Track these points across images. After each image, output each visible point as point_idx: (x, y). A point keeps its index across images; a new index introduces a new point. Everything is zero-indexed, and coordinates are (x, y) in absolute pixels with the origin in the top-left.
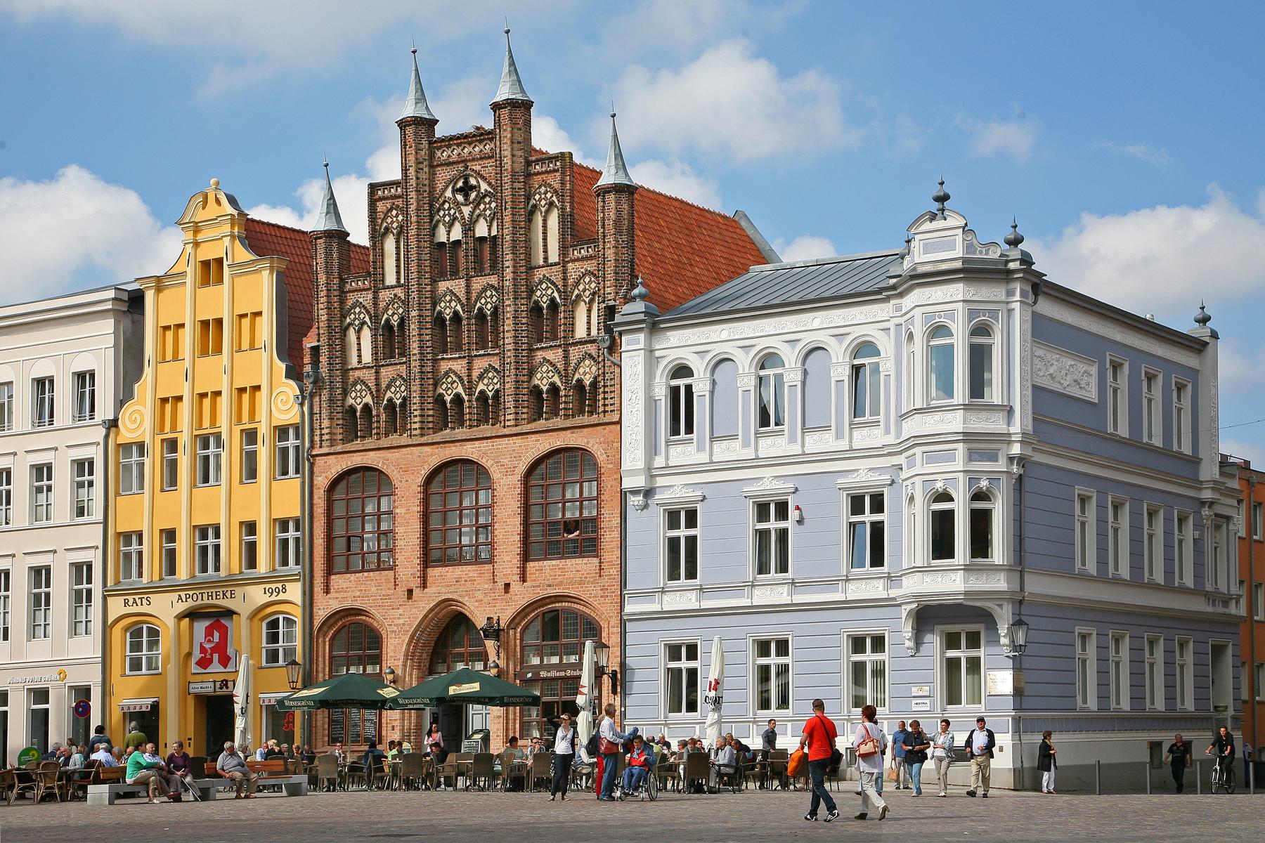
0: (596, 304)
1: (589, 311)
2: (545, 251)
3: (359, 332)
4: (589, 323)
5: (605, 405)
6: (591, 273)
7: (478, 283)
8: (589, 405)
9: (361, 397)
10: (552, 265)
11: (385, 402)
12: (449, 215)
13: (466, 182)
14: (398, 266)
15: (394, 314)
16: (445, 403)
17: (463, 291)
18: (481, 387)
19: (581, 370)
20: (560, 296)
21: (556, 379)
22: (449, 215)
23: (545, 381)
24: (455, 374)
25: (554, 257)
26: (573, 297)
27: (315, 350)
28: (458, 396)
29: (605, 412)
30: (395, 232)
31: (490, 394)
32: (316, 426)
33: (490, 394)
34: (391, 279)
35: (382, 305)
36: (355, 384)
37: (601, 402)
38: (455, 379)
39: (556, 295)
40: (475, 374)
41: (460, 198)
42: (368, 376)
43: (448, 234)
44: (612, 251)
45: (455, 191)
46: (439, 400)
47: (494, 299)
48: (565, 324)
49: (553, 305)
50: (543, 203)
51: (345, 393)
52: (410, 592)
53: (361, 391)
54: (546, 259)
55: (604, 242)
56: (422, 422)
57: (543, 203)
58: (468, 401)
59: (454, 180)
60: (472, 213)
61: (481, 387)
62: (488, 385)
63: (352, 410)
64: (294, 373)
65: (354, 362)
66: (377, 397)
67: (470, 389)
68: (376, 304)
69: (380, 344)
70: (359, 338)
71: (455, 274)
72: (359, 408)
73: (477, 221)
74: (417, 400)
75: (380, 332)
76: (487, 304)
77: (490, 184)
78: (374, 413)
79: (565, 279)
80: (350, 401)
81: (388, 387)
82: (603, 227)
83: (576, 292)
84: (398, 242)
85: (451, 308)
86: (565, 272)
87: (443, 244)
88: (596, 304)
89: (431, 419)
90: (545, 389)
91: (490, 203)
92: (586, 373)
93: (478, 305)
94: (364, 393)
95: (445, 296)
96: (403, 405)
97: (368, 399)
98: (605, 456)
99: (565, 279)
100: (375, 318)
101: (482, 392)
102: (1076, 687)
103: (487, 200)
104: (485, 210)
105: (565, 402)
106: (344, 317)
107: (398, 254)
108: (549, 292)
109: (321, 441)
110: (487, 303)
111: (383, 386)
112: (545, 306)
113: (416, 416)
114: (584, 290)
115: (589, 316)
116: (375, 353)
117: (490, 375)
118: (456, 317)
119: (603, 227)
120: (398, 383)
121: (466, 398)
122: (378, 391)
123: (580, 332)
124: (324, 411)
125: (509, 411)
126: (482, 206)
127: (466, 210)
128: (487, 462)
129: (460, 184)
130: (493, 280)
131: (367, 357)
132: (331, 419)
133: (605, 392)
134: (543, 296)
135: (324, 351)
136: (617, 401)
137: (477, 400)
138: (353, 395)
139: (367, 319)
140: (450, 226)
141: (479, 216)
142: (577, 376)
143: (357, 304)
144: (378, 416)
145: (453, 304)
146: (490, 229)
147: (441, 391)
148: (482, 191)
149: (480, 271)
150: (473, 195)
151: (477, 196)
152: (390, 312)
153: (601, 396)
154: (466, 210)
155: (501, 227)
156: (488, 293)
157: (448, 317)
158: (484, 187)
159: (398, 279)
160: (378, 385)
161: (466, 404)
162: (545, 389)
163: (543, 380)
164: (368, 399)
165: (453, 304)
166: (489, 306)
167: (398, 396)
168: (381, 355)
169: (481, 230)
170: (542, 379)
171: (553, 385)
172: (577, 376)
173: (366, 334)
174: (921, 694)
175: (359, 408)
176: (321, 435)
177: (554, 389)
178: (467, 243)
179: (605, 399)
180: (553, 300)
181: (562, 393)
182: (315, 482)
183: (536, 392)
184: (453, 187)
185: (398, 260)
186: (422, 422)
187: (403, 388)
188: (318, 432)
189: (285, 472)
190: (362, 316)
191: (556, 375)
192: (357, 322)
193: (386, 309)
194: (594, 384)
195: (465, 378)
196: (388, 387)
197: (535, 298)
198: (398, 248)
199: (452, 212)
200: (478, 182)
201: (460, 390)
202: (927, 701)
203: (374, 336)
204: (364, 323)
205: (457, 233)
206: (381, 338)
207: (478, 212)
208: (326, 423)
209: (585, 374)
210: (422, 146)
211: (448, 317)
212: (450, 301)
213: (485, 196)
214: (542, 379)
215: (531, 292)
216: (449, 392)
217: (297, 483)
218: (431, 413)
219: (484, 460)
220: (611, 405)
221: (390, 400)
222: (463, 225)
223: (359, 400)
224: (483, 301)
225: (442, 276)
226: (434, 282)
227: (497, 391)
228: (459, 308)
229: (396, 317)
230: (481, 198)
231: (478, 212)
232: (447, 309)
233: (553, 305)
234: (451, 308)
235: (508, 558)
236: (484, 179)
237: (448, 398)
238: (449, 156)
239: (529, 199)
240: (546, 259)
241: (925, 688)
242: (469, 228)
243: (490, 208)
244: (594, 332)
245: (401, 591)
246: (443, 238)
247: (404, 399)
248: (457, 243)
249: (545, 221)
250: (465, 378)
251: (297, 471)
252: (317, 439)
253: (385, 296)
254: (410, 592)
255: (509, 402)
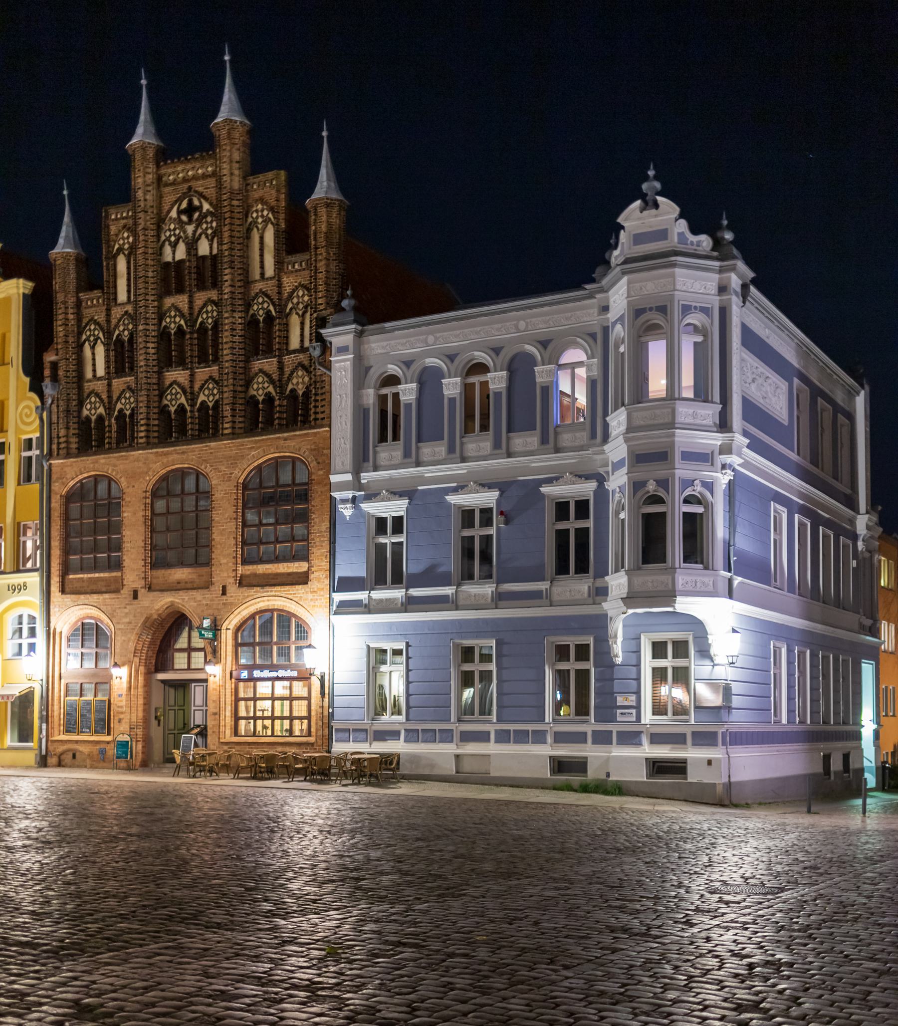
0: (309, 314)
1: (302, 324)
2: (262, 267)
3: (93, 348)
4: (302, 335)
5: (316, 413)
6: (304, 287)
7: (200, 298)
8: (301, 415)
9: (96, 409)
10: (267, 279)
11: (116, 413)
12: (175, 235)
13: (190, 202)
14: (129, 285)
15: (124, 330)
16: (169, 412)
17: (186, 306)
18: (202, 398)
19: (295, 381)
20: (275, 309)
21: (271, 389)
22: (175, 235)
23: (261, 392)
24: (179, 385)
25: (270, 271)
26: (288, 310)
27: (54, 366)
28: (181, 409)
29: (316, 419)
30: (126, 252)
31: (211, 405)
32: (54, 434)
33: (211, 405)
34: (122, 296)
35: (114, 322)
36: (89, 396)
37: (313, 410)
38: (179, 390)
39: (271, 308)
40: (197, 387)
41: (184, 218)
42: (100, 386)
43: (174, 253)
44: (323, 263)
45: (180, 212)
46: (163, 411)
47: (215, 314)
48: (279, 337)
49: (269, 317)
50: (260, 220)
51: (81, 404)
52: (135, 595)
53: (95, 402)
54: (262, 274)
55: (316, 255)
56: (147, 431)
57: (260, 220)
58: (191, 411)
59: (179, 200)
60: (195, 232)
61: (202, 398)
62: (208, 396)
63: (88, 419)
64: (36, 387)
65: (89, 375)
66: (110, 408)
67: (192, 399)
68: (108, 321)
69: (112, 359)
70: (93, 354)
71: (180, 290)
72: (93, 418)
73: (199, 238)
74: (143, 410)
75: (112, 347)
76: (207, 318)
77: (211, 204)
78: (107, 423)
79: (279, 293)
80: (85, 412)
81: (119, 399)
82: (315, 239)
83: (290, 306)
84: (128, 263)
85: (175, 322)
86: (280, 286)
87: (168, 263)
88: (309, 314)
89: (156, 428)
90: (261, 399)
91: (211, 222)
92: (299, 382)
93: (200, 320)
94: (98, 405)
95: (169, 310)
96: (132, 416)
97: (101, 410)
98: (315, 462)
99: (279, 293)
100: (108, 334)
101: (203, 402)
102: (770, 688)
103: (209, 219)
104: (207, 229)
105: (279, 412)
106: (80, 333)
107: (129, 274)
108: (265, 305)
109: (59, 449)
110: (208, 318)
111: (115, 398)
112: (261, 319)
113: (142, 425)
114: (298, 303)
115: (302, 329)
116: (107, 367)
117: (211, 386)
118: (180, 331)
119: (315, 239)
120: (128, 395)
121: (188, 408)
122: (110, 403)
123: (295, 343)
124: (61, 421)
125: (226, 420)
126: (204, 226)
127: (190, 229)
128: (206, 468)
129: (184, 205)
130: (213, 295)
131: (101, 371)
132: (68, 428)
133: (316, 401)
134: (260, 308)
135: (62, 364)
136: (326, 409)
137: (199, 410)
138: (89, 406)
139: (101, 335)
140: (174, 246)
141: (200, 235)
142: (290, 387)
143: (92, 320)
144: (110, 426)
145: (178, 319)
146: (211, 248)
147: (166, 402)
148: (204, 210)
149: (201, 287)
150: (196, 215)
151: (199, 216)
152: (121, 328)
153: (313, 404)
154: (190, 229)
155: (220, 244)
156: (209, 308)
157: (173, 332)
158: (206, 206)
159: (129, 297)
160: (110, 397)
161: (189, 414)
162: (261, 399)
163: (260, 388)
164: (101, 410)
165: (178, 319)
166: (210, 321)
167: (128, 407)
168: (112, 370)
169: (204, 248)
170: (258, 389)
171: (268, 395)
172: (290, 387)
173: (100, 350)
174: (626, 703)
175: (93, 418)
176: (59, 443)
177: (269, 399)
178: (189, 261)
179: (316, 407)
180: (268, 313)
181: (277, 403)
182: (53, 488)
183: (252, 402)
184: (178, 208)
185: (129, 280)
186: (147, 431)
187: (132, 400)
188: (56, 441)
189: (28, 479)
190: (96, 333)
191: (271, 386)
192: (92, 338)
193: (117, 326)
194: (306, 394)
195: (188, 390)
196: (119, 399)
197: (251, 312)
198: (129, 268)
199: (177, 232)
200: (201, 203)
201: (183, 400)
202: (634, 711)
203: (107, 351)
204: (99, 338)
205: (181, 253)
206: (112, 353)
207: (199, 231)
208: (62, 432)
209: (298, 383)
210: (150, 170)
211: (173, 332)
212: (175, 316)
213: (206, 217)
214: (258, 389)
215: (248, 306)
216: (174, 402)
217: (37, 486)
218: (156, 422)
219: (203, 467)
220: (322, 413)
221: (121, 411)
222: (187, 244)
223: (93, 412)
224: (205, 316)
225: (168, 293)
226: (160, 298)
227: (217, 402)
228: (182, 322)
229: (126, 333)
230: (203, 216)
231: (199, 231)
232: (173, 322)
233: (269, 317)
234: (175, 322)
235: (225, 561)
236: (206, 199)
237: (173, 409)
238: (175, 180)
239: (247, 217)
240: (262, 274)
241: (630, 698)
242: (192, 245)
243: (212, 228)
244: (307, 344)
245: (126, 592)
246: (169, 258)
247: (133, 410)
248: (182, 262)
249: (262, 238)
250: (188, 390)
251: (37, 479)
252: (54, 447)
253: (117, 312)
254: (135, 595)
255: (227, 411)
